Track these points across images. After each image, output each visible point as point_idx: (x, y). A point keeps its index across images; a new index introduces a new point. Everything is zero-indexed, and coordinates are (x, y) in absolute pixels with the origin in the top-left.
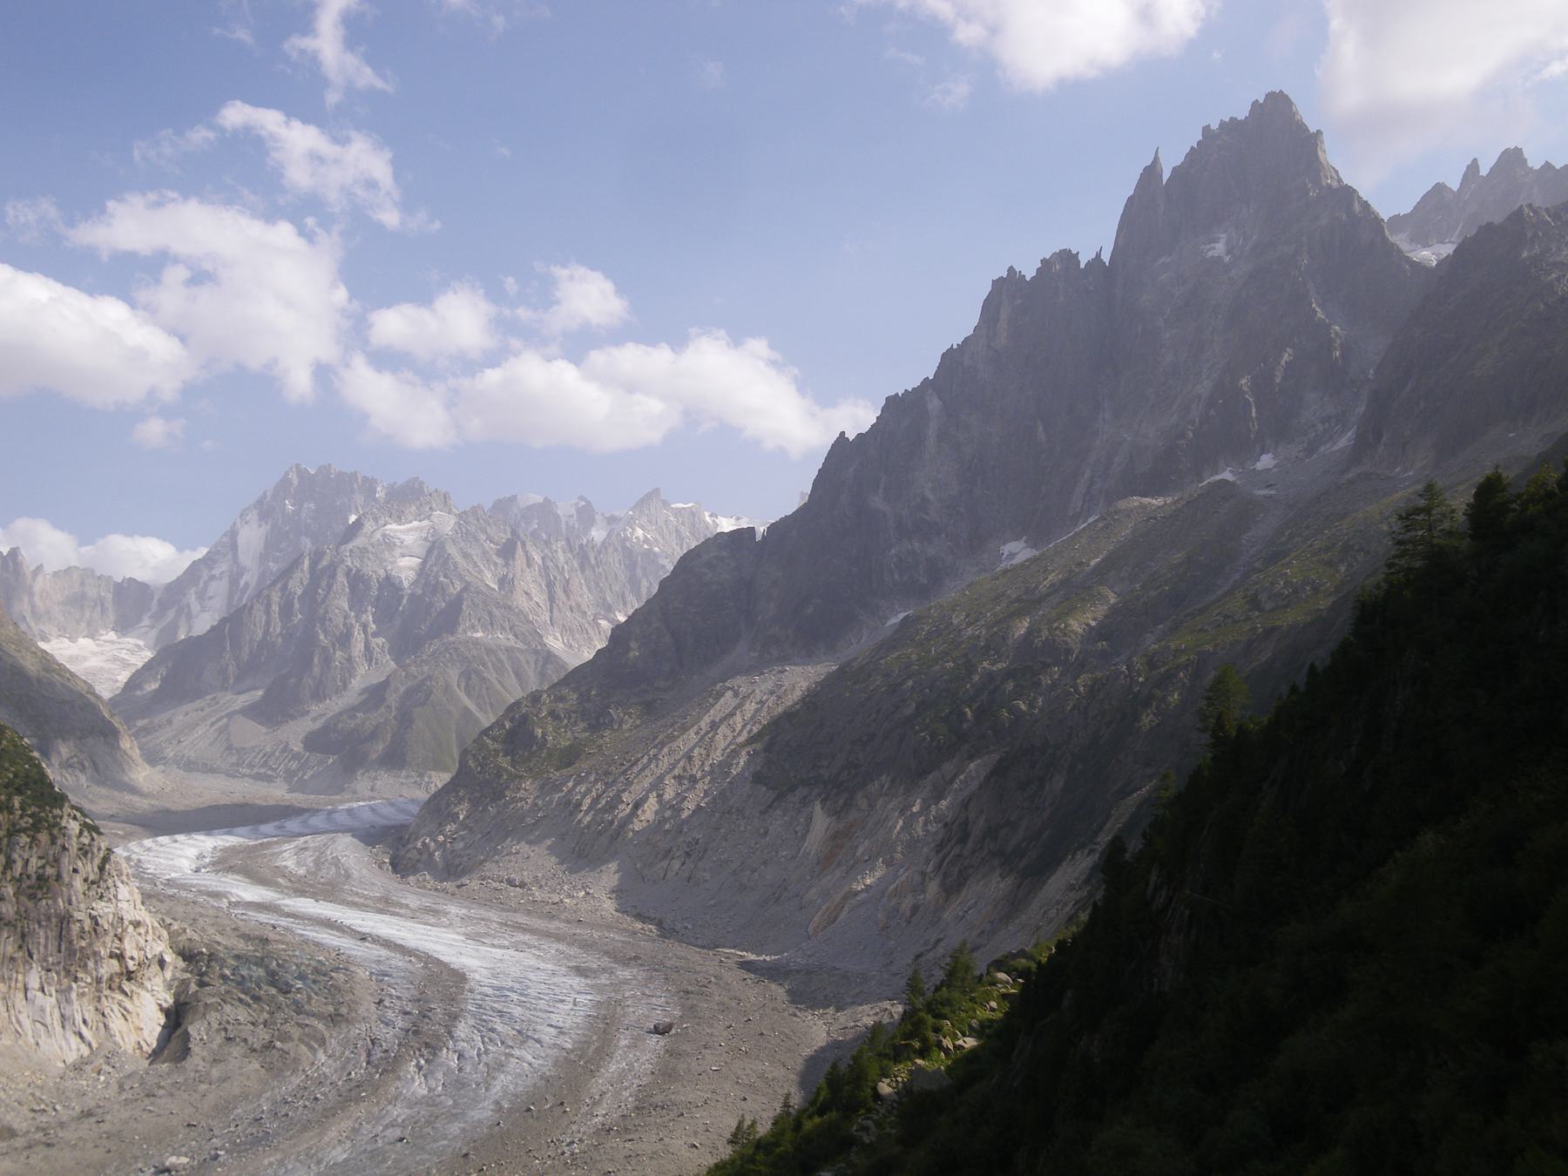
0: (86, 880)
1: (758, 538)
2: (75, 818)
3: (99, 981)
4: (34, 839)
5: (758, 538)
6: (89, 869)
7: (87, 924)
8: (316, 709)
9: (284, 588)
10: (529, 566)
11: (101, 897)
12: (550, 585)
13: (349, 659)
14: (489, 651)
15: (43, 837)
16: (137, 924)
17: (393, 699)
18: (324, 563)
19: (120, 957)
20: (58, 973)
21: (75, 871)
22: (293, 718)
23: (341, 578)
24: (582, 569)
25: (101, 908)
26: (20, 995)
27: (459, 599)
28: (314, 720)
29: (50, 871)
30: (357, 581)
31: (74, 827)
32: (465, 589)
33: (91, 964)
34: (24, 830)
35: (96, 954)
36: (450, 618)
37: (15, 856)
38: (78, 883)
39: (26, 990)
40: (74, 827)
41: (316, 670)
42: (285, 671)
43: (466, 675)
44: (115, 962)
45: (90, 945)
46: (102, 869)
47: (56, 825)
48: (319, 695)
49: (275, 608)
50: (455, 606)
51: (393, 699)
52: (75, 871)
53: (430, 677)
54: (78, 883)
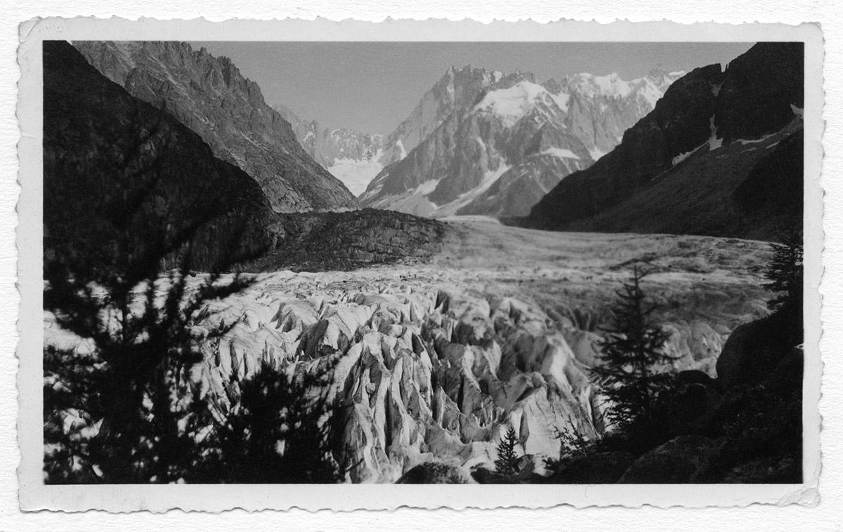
1: (723, 70)
5: (723, 70)
8: (462, 196)
9: (444, 131)
10: (581, 112)
12: (594, 123)
13: (480, 169)
18: (466, 116)
22: (450, 201)
23: (474, 123)
27: (541, 132)
28: (461, 202)
30: (485, 127)
32: (544, 126)
36: (536, 146)
41: (462, 175)
48: (464, 190)
49: (440, 142)
50: (538, 136)
51: (503, 189)
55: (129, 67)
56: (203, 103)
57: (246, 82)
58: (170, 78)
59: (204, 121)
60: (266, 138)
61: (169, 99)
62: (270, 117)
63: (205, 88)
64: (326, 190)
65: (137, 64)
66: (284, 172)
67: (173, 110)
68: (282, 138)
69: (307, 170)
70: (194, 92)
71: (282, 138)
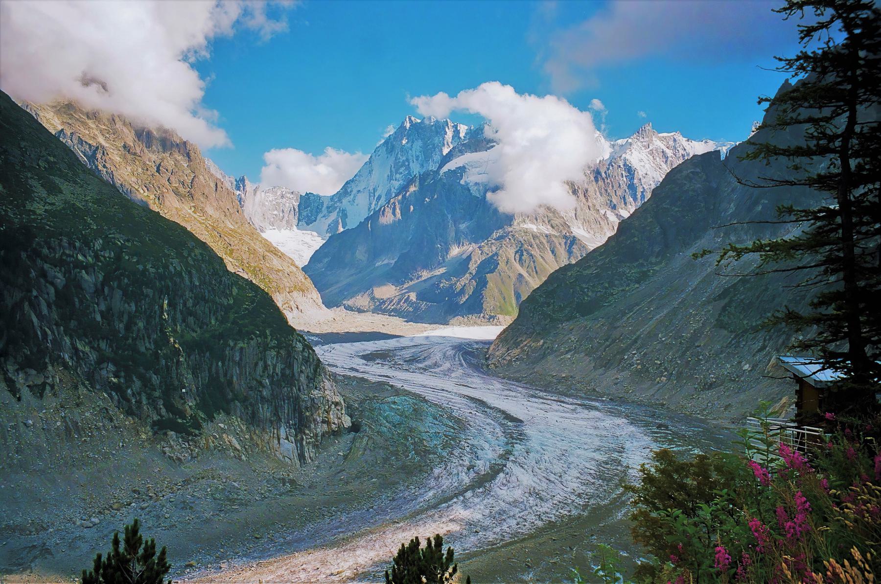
0: (308, 377)
2: (300, 341)
3: (316, 435)
4: (278, 353)
6: (309, 371)
7: (309, 404)
11: (316, 388)
14: (535, 237)
15: (283, 352)
16: (337, 404)
17: (473, 267)
19: (327, 422)
20: (295, 429)
21: (301, 372)
24: (597, 181)
25: (316, 393)
26: (276, 441)
29: (288, 372)
31: (300, 346)
33: (313, 426)
34: (273, 348)
35: (315, 420)
37: (269, 363)
38: (303, 378)
39: (279, 440)
40: (300, 346)
42: (404, 251)
43: (520, 252)
44: (325, 426)
45: (312, 415)
46: (315, 371)
47: (291, 345)
51: (473, 267)
52: (301, 372)
53: (496, 254)
54: (303, 378)
55: (55, 127)
56: (140, 170)
57: (185, 143)
58: (101, 140)
59: (142, 191)
60: (210, 211)
61: (104, 166)
62: (213, 185)
63: (138, 151)
64: (278, 271)
65: (63, 123)
66: (232, 251)
67: (110, 180)
68: (226, 210)
69: (256, 247)
70: (129, 157)
71: (226, 210)
